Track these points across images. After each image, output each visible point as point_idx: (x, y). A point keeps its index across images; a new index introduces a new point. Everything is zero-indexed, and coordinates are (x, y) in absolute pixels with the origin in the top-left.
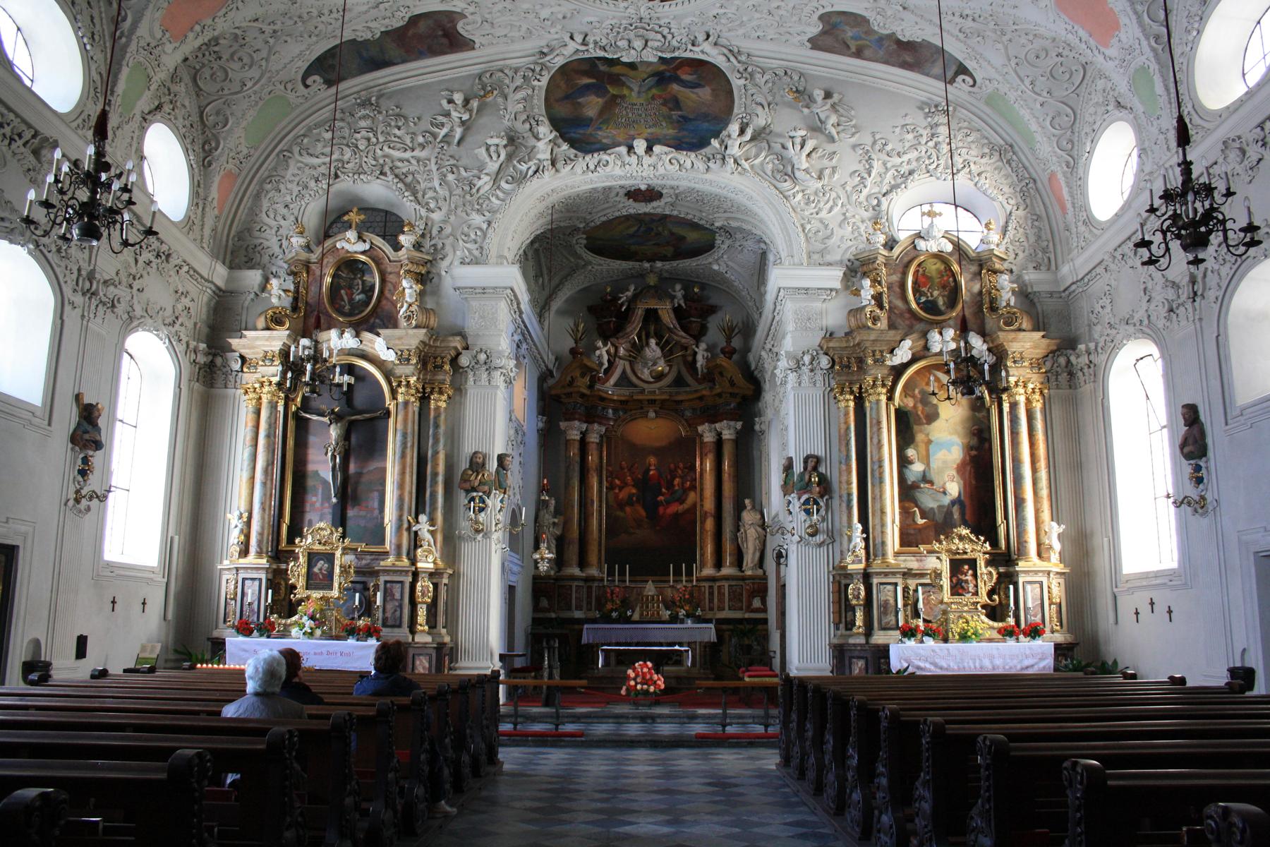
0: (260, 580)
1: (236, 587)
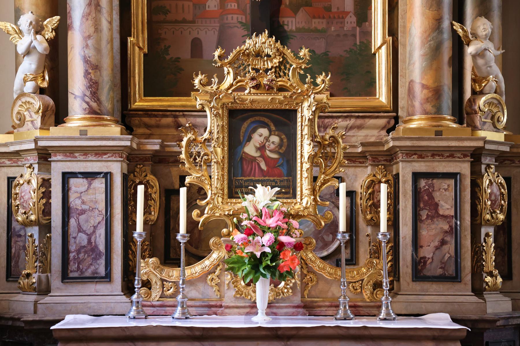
0: (108, 176)
1: (47, 195)
